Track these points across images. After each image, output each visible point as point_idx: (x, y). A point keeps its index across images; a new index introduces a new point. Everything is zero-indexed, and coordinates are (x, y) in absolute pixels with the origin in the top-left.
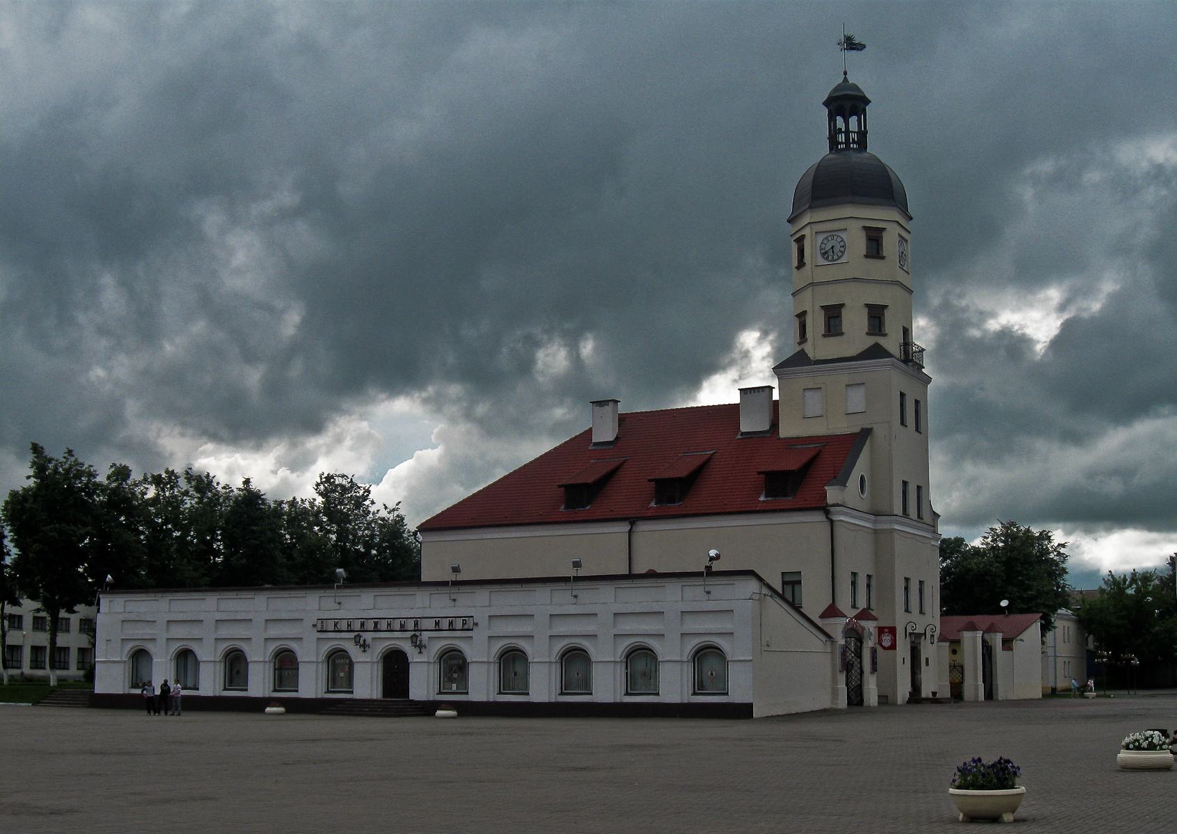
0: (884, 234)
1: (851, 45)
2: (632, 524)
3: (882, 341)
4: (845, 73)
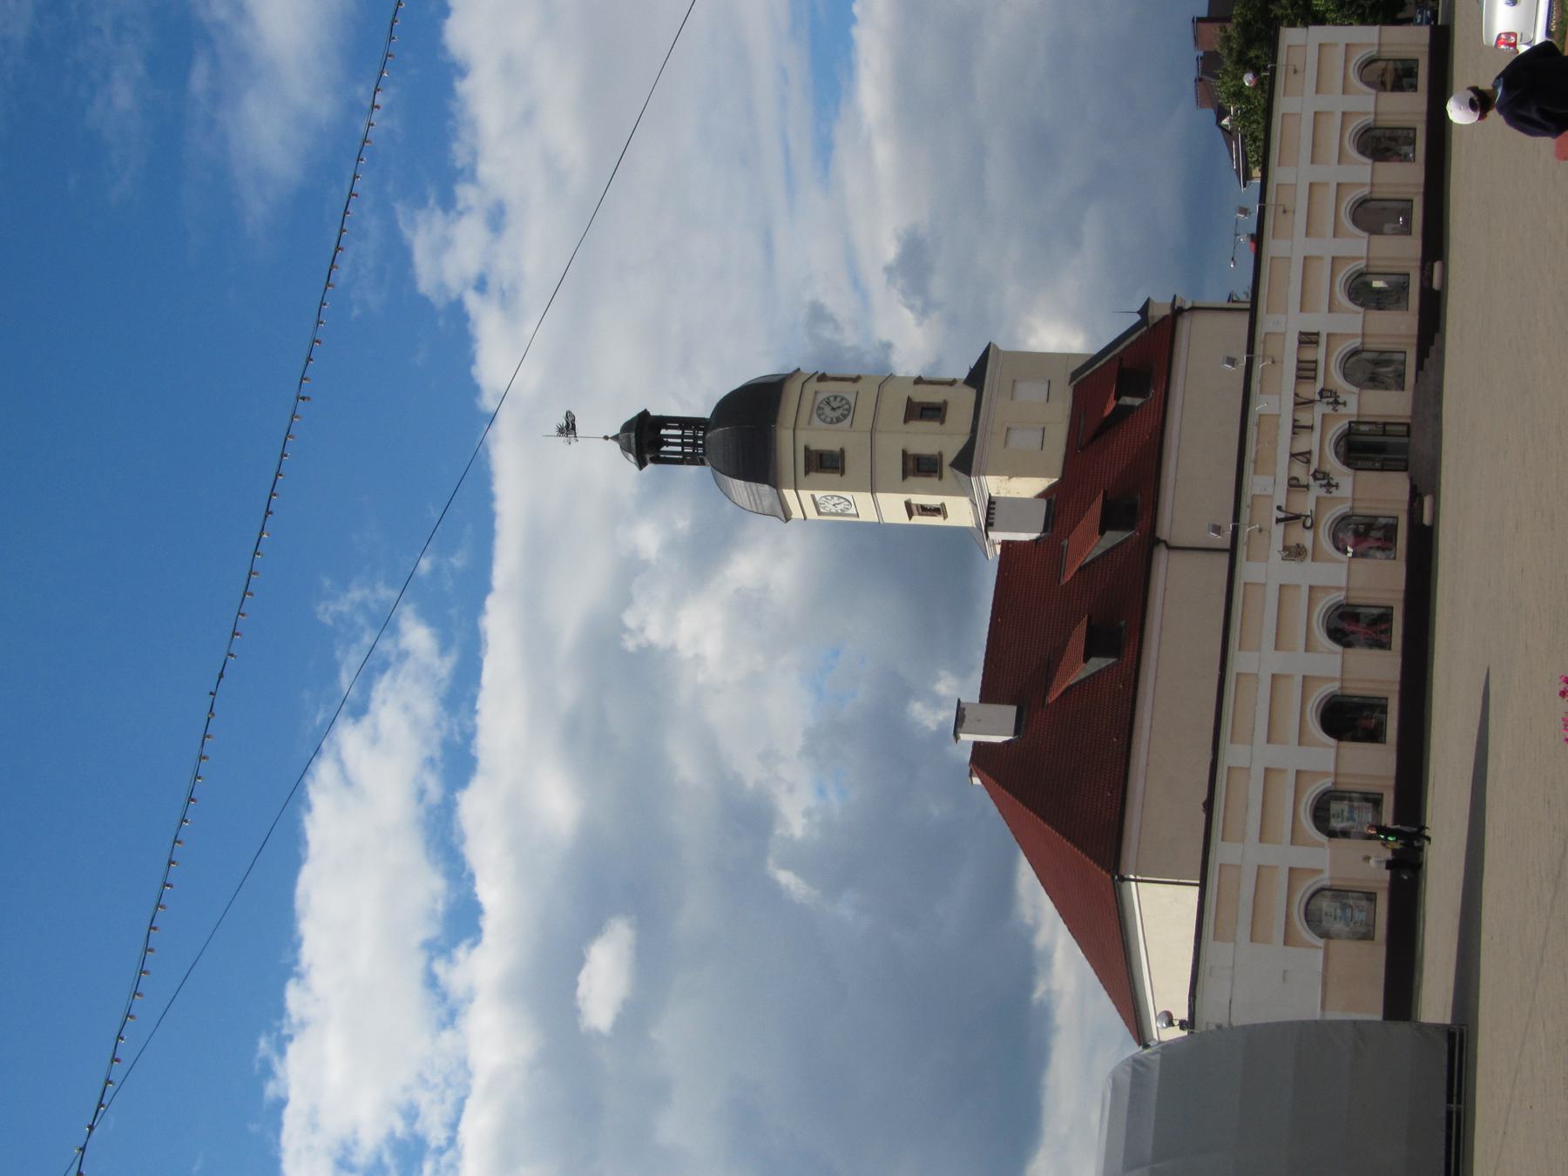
0: (813, 447)
1: (569, 428)
2: (1158, 541)
3: (949, 457)
4: (606, 438)
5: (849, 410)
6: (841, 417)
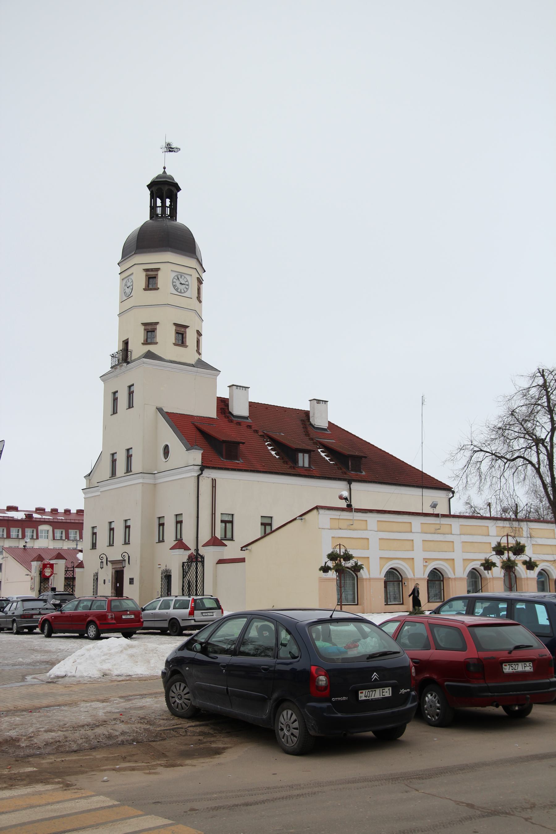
1: (170, 149)
4: (164, 168)
5: (181, 292)
6: (176, 288)
